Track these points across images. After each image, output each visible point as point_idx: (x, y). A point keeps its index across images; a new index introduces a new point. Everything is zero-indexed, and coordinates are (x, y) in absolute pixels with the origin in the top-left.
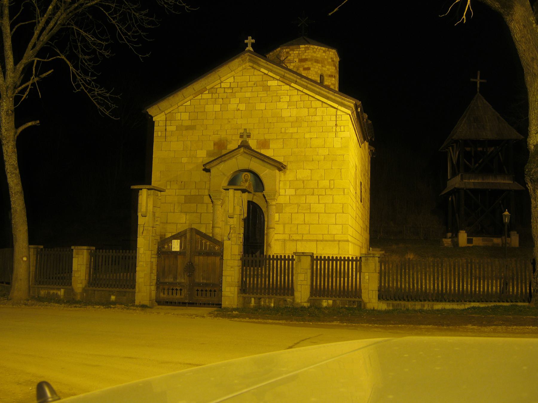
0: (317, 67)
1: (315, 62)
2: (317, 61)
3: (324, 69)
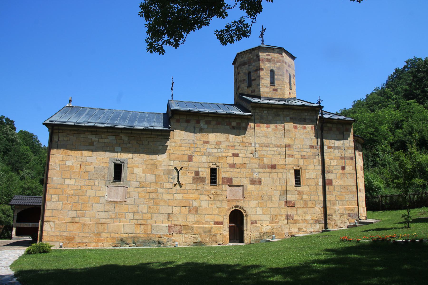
0: (245, 69)
1: (243, 65)
2: (244, 64)
3: (251, 67)
